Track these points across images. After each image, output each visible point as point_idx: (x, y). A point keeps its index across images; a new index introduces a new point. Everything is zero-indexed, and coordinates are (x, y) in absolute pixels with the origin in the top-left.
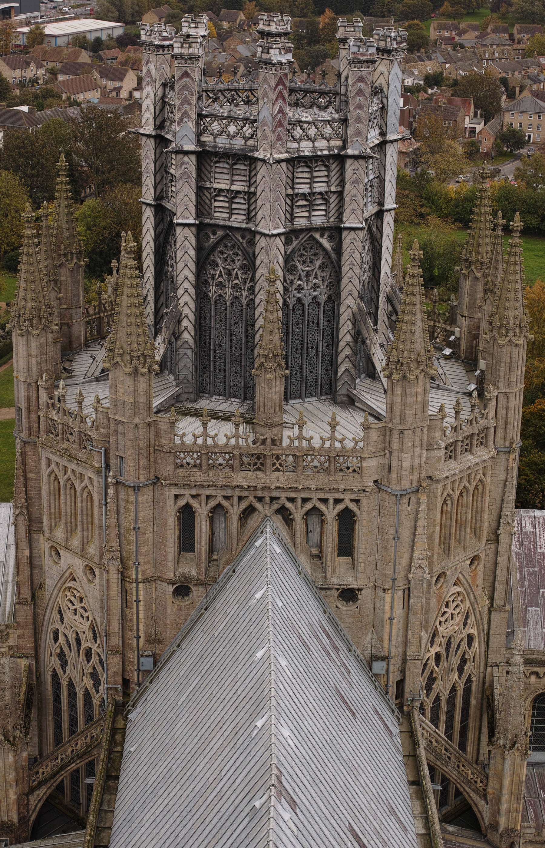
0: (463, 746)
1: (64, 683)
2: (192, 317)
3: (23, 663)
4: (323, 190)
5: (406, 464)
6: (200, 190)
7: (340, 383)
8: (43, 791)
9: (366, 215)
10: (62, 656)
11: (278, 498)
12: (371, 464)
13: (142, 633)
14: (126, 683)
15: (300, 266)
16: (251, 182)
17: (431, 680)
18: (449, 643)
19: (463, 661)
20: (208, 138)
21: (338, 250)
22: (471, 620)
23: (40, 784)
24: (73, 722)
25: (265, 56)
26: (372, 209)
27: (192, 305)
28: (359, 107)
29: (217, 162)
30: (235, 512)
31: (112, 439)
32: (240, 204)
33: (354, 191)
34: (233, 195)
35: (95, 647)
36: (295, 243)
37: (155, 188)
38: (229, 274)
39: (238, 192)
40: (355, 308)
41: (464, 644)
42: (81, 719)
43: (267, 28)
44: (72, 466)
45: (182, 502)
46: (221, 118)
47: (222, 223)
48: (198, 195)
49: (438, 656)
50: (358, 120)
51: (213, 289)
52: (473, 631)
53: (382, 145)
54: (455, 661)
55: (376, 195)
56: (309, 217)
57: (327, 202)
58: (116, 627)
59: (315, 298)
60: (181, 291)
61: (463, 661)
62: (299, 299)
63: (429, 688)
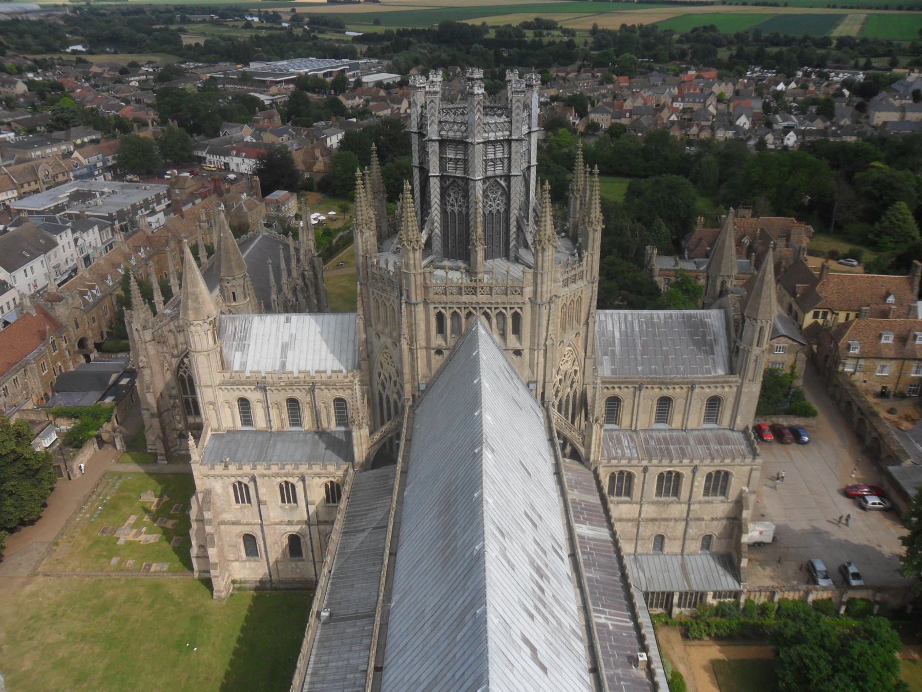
0: (573, 422)
1: (384, 397)
2: (439, 221)
4: (501, 157)
5: (545, 289)
6: (441, 159)
7: (511, 252)
9: (522, 168)
10: (383, 384)
11: (483, 308)
13: (420, 373)
15: (490, 195)
16: (465, 154)
17: (557, 391)
18: (566, 374)
19: (572, 382)
20: (443, 133)
21: (509, 186)
22: (576, 363)
25: (471, 91)
26: (525, 165)
27: (439, 215)
28: (518, 115)
30: (463, 314)
32: (460, 165)
33: (516, 157)
34: (456, 161)
36: (488, 183)
37: (419, 158)
38: (457, 200)
39: (459, 159)
41: (573, 375)
42: (393, 413)
43: (471, 76)
45: (437, 311)
46: (450, 122)
47: (452, 174)
48: (440, 161)
49: (560, 381)
50: (517, 121)
51: (449, 207)
52: (577, 368)
53: (529, 133)
54: (569, 383)
55: (527, 158)
56: (494, 171)
57: (503, 163)
59: (498, 210)
60: (433, 209)
61: (572, 382)
62: (490, 211)
63: (556, 395)
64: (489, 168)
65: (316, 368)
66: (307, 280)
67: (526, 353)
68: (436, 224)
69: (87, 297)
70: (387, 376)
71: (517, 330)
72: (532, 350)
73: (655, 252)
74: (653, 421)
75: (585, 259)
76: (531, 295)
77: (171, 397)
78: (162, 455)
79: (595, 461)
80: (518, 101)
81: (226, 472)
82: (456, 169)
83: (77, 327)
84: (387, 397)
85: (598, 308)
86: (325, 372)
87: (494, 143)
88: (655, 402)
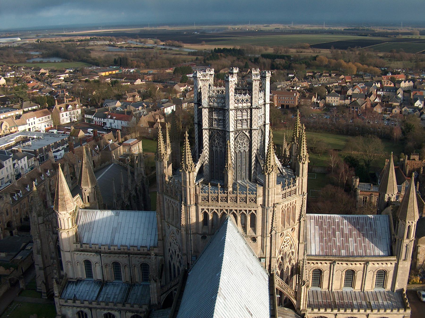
1: (172, 264)
3: (160, 258)
5: (270, 199)
8: (165, 295)
10: (171, 256)
13: (192, 249)
14: (188, 264)
15: (239, 141)
16: (224, 116)
19: (290, 259)
20: (211, 104)
22: (293, 247)
23: (164, 293)
24: (175, 276)
27: (208, 153)
35: (180, 254)
38: (219, 144)
39: (221, 119)
41: (291, 254)
44: (172, 200)
51: (214, 148)
52: (293, 250)
54: (288, 260)
55: (263, 119)
58: (185, 247)
60: (204, 149)
61: (290, 259)
64: (238, 125)
65: (132, 244)
66: (138, 192)
67: (259, 239)
68: (206, 158)
69: (14, 197)
70: (174, 251)
71: (253, 225)
72: (263, 236)
73: (358, 180)
74: (343, 285)
75: (297, 181)
76: (262, 203)
77: (52, 258)
78: (44, 293)
79: (303, 310)
81: (74, 304)
83: (7, 214)
84: (174, 264)
85: (307, 212)
86: (136, 247)
87: (242, 110)
88: (344, 272)
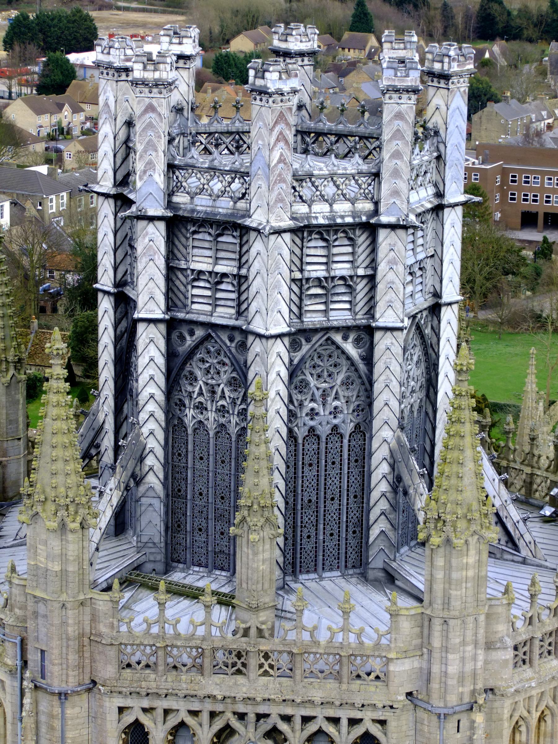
2: (160, 452)
4: (345, 273)
5: (453, 669)
7: (372, 552)
9: (411, 309)
11: (267, 716)
12: (402, 668)
15: (313, 382)
20: (180, 199)
25: (259, 82)
27: (160, 435)
28: (397, 155)
29: (194, 232)
31: (30, 624)
33: (391, 276)
36: (306, 347)
37: (116, 269)
39: (224, 275)
40: (393, 444)
43: (283, 46)
45: (129, 719)
46: (224, 173)
47: (202, 318)
48: (169, 279)
51: (190, 413)
53: (438, 209)
56: (326, 312)
57: (351, 290)
59: (335, 428)
60: (143, 416)
62: (312, 430)
64: (310, 305)
68: (150, 461)
80: (399, 116)
82: (215, 303)
